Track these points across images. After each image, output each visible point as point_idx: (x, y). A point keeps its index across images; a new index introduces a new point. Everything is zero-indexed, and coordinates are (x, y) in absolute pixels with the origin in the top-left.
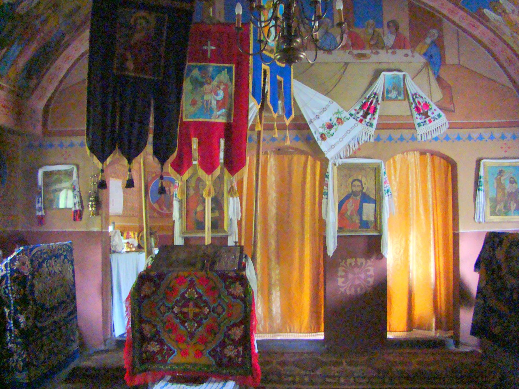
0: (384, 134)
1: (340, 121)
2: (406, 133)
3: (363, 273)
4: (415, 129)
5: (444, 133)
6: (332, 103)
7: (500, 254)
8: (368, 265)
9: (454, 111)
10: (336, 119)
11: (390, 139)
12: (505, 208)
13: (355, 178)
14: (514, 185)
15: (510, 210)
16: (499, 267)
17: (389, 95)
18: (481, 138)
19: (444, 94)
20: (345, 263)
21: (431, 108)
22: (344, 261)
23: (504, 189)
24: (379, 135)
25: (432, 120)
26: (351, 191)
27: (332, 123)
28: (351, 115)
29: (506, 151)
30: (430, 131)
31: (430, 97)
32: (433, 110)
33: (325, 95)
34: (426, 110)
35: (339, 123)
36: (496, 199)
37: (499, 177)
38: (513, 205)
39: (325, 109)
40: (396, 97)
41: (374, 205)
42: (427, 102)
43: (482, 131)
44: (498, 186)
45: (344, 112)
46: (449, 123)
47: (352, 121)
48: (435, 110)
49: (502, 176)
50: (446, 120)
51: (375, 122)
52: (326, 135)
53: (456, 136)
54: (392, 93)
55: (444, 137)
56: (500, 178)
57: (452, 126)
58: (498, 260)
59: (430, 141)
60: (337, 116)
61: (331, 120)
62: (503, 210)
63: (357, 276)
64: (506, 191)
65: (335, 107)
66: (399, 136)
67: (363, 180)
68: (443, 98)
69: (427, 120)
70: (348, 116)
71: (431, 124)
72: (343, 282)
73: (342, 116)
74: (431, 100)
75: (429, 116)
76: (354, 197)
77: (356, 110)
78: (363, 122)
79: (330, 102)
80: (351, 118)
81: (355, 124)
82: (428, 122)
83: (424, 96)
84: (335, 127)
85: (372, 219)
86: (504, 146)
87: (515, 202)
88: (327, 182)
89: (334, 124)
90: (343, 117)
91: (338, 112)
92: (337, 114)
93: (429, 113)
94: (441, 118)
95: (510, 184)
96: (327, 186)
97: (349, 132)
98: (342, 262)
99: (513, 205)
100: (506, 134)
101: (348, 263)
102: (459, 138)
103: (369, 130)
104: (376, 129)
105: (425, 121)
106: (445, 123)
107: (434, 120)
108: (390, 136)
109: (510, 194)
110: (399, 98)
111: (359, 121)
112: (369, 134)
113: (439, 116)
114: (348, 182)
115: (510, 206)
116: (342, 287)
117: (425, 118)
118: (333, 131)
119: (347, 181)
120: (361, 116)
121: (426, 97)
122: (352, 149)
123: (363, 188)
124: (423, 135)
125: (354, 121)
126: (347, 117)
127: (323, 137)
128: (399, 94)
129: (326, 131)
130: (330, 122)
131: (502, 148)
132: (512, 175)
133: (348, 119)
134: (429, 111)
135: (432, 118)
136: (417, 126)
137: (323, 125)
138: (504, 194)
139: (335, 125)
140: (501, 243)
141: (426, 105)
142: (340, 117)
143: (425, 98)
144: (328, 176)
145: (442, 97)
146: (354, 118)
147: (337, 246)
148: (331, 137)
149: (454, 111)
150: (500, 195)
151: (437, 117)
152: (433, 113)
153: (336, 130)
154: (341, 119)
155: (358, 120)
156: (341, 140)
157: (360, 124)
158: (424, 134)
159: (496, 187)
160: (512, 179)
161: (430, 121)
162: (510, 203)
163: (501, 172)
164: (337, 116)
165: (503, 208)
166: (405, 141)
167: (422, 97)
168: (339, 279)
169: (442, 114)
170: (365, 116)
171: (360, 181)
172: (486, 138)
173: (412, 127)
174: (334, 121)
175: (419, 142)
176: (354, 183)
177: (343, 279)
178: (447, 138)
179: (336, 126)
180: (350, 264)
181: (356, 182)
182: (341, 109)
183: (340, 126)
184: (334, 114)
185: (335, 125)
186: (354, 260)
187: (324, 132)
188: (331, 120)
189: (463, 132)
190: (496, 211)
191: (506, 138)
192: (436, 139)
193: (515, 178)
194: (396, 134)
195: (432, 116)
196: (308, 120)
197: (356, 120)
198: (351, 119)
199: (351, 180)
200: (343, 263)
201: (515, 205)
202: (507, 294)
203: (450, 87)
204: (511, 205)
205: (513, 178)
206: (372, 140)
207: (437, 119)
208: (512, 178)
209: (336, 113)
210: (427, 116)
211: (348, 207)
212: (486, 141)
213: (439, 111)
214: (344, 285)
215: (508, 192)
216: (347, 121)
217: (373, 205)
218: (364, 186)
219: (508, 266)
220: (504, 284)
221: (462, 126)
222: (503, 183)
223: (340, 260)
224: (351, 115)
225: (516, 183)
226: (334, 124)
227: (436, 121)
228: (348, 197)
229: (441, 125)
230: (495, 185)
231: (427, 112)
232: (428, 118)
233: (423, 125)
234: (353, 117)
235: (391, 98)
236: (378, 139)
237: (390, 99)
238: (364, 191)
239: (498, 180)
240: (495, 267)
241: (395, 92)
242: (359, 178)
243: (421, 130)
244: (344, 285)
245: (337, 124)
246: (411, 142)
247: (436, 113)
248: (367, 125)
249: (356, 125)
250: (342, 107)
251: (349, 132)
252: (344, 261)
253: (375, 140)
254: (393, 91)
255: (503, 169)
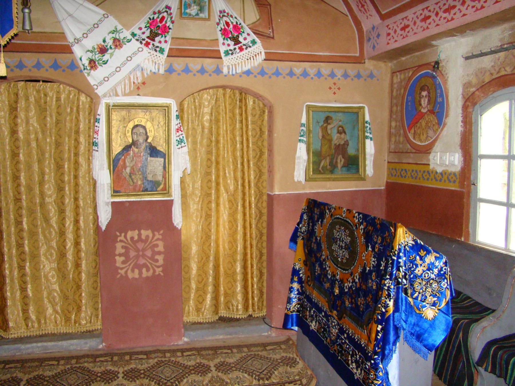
0: (179, 63)
1: (118, 43)
2: (209, 63)
3: (150, 250)
4: (221, 58)
5: (259, 65)
6: (108, 17)
7: (320, 231)
8: (155, 238)
9: (273, 38)
10: (112, 41)
11: (187, 70)
12: (331, 163)
13: (136, 123)
14: (343, 135)
15: (337, 167)
16: (319, 245)
17: (188, 11)
18: (305, 74)
19: (261, 13)
20: (125, 237)
21: (243, 32)
22: (123, 234)
23: (330, 141)
24: (171, 64)
25: (244, 47)
26: (131, 141)
27: (107, 46)
28: (133, 35)
29: (335, 93)
30: (237, 63)
31: (242, 17)
32: (244, 35)
33: (97, 6)
34: (236, 34)
35: (116, 46)
36: (321, 152)
37: (325, 125)
38: (341, 161)
39: (96, 26)
40: (197, 14)
41: (162, 160)
42: (239, 24)
43: (306, 65)
44: (323, 137)
45: (124, 30)
46: (265, 52)
47: (135, 45)
48: (248, 34)
49: (329, 124)
50: (262, 49)
51: (167, 47)
52: (97, 63)
53: (274, 70)
54: (192, 8)
55: (259, 70)
56: (326, 127)
57: (269, 58)
58: (318, 238)
59: (241, 76)
60: (114, 35)
61: (104, 41)
62: (328, 167)
63: (141, 253)
64: (333, 143)
65: (112, 22)
66: (199, 67)
67: (149, 126)
68: (259, 19)
69: (237, 47)
70: (130, 37)
71: (242, 53)
72: (123, 262)
73: (122, 36)
74: (244, 22)
75: (240, 43)
76: (136, 150)
77: (140, 29)
78: (151, 46)
79: (104, 15)
80: (133, 39)
81: (139, 48)
82: (238, 50)
83: (235, 15)
84: (110, 51)
85: (160, 178)
86: (333, 87)
87: (343, 158)
88: (97, 128)
89: (109, 47)
90: (122, 38)
91: (115, 31)
92: (113, 33)
93: (241, 39)
94: (256, 46)
95: (338, 135)
96: (97, 133)
97: (129, 59)
98: (121, 236)
99: (341, 161)
100: (336, 71)
101: (128, 237)
102: (277, 73)
103: (158, 56)
104: (168, 56)
105: (235, 49)
106: (261, 52)
107: (246, 48)
108: (21, 61)
109: (337, 147)
110: (202, 15)
111: (145, 45)
112: (157, 62)
113: (254, 42)
114: (127, 129)
115: (337, 162)
116: (122, 269)
117: (235, 45)
118: (106, 57)
119: (125, 127)
120: (148, 37)
121: (236, 16)
122: (134, 83)
123: (147, 138)
124: (231, 67)
125: (138, 43)
126: (128, 38)
127: (93, 64)
128: (201, 10)
129: (97, 56)
130: (103, 44)
131: (330, 88)
132: (340, 123)
133: (129, 41)
134: (240, 36)
135: (244, 45)
136: (223, 55)
137: (93, 47)
138: (330, 147)
139: (111, 48)
140: (322, 216)
141: (237, 28)
142: (118, 37)
143: (236, 18)
144: (99, 119)
145: (258, 17)
146: (137, 40)
147: (112, 216)
148: (103, 65)
149: (273, 38)
150: (325, 149)
151: (251, 45)
152: (245, 39)
153: (112, 55)
154: (119, 41)
155: (144, 42)
156: (118, 69)
157: (145, 49)
158: (232, 65)
159: (321, 138)
160: (340, 128)
161: (241, 49)
162: (337, 159)
163: (327, 120)
164: (114, 35)
165: (328, 164)
166: (206, 75)
167: (232, 16)
168: (117, 258)
169: (257, 40)
170: (152, 37)
171: (144, 128)
172: (312, 76)
173: (216, 55)
174: (110, 42)
175: (226, 76)
176: (134, 131)
177: (123, 258)
178: (262, 73)
179: (112, 51)
180: (132, 238)
181: (138, 128)
182: (120, 27)
183: (117, 50)
184: (110, 33)
185: (111, 48)
186: (137, 232)
187: (94, 58)
188: (104, 41)
189: (284, 66)
190: (320, 169)
191: (336, 76)
192: (248, 73)
193: (345, 127)
194: (195, 64)
195: (244, 42)
196: (71, 39)
197: (141, 43)
198: (134, 40)
199: (131, 125)
200: (122, 238)
201: (343, 160)
202: (327, 285)
203: (270, 5)
204: (339, 161)
205: (342, 127)
206: (162, 71)
207: (250, 47)
208: (340, 127)
209: (113, 32)
210: (236, 41)
211: (128, 164)
212: (312, 78)
213: (254, 37)
214: (124, 266)
215: (335, 145)
216: (127, 44)
217: (162, 160)
218: (148, 134)
219: (329, 248)
220: (323, 270)
221: (282, 58)
222: (329, 132)
223: (118, 234)
224: (133, 35)
225: (345, 133)
226: (109, 47)
227: (249, 49)
228: (127, 148)
229: (256, 55)
230: (320, 134)
231: (238, 36)
232: (239, 45)
233: (232, 54)
234: (137, 38)
235: (190, 15)
236: (170, 70)
237: (190, 17)
238: (149, 140)
239: (325, 129)
240: (314, 246)
241: (195, 7)
242: (143, 124)
243: (227, 61)
244: (124, 266)
245: (113, 47)
246: (214, 75)
247: (249, 39)
248: (156, 51)
249: (140, 50)
250: (120, 23)
251: (129, 59)
252: (123, 234)
253: (166, 71)
254: (193, 5)
255: (330, 115)
